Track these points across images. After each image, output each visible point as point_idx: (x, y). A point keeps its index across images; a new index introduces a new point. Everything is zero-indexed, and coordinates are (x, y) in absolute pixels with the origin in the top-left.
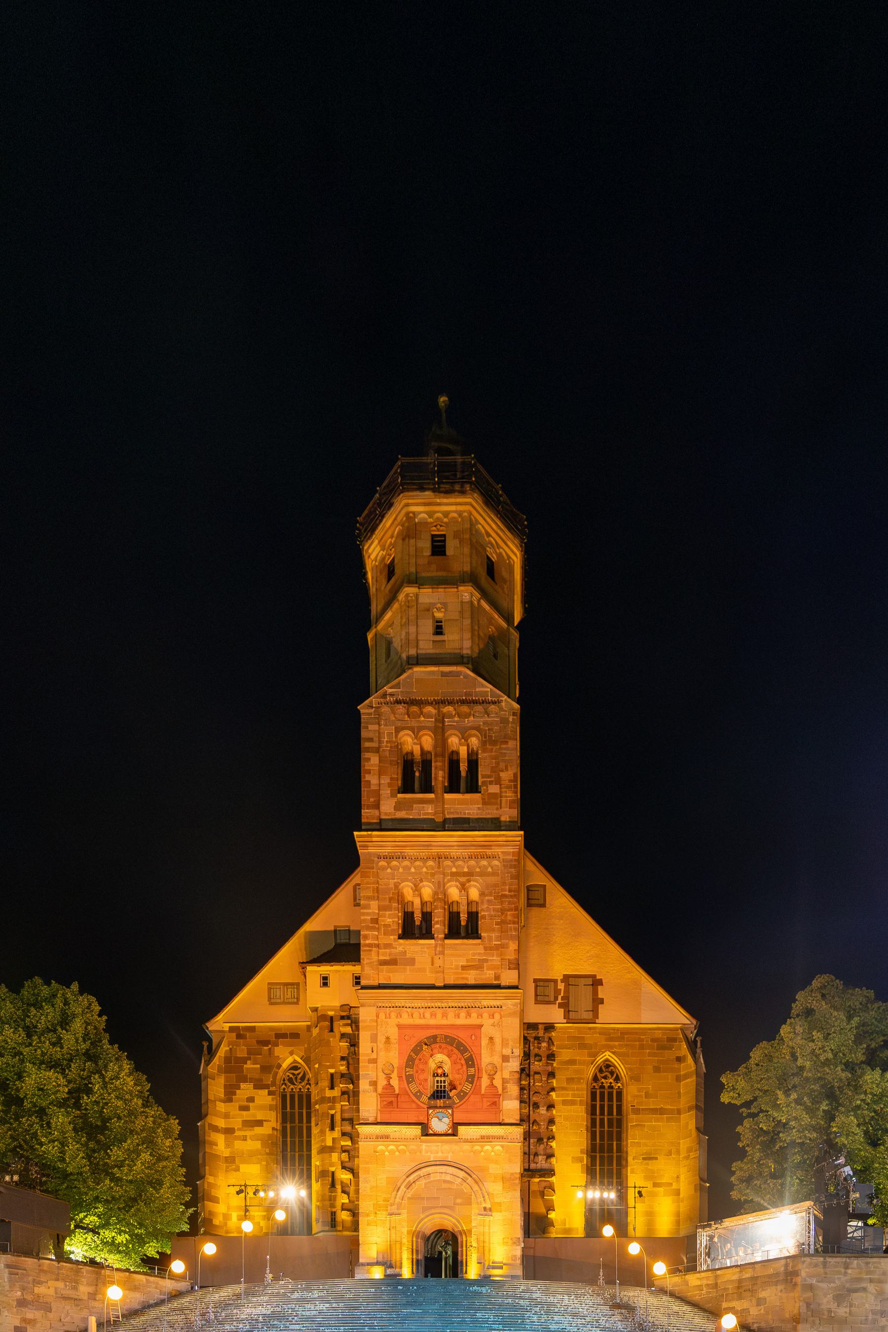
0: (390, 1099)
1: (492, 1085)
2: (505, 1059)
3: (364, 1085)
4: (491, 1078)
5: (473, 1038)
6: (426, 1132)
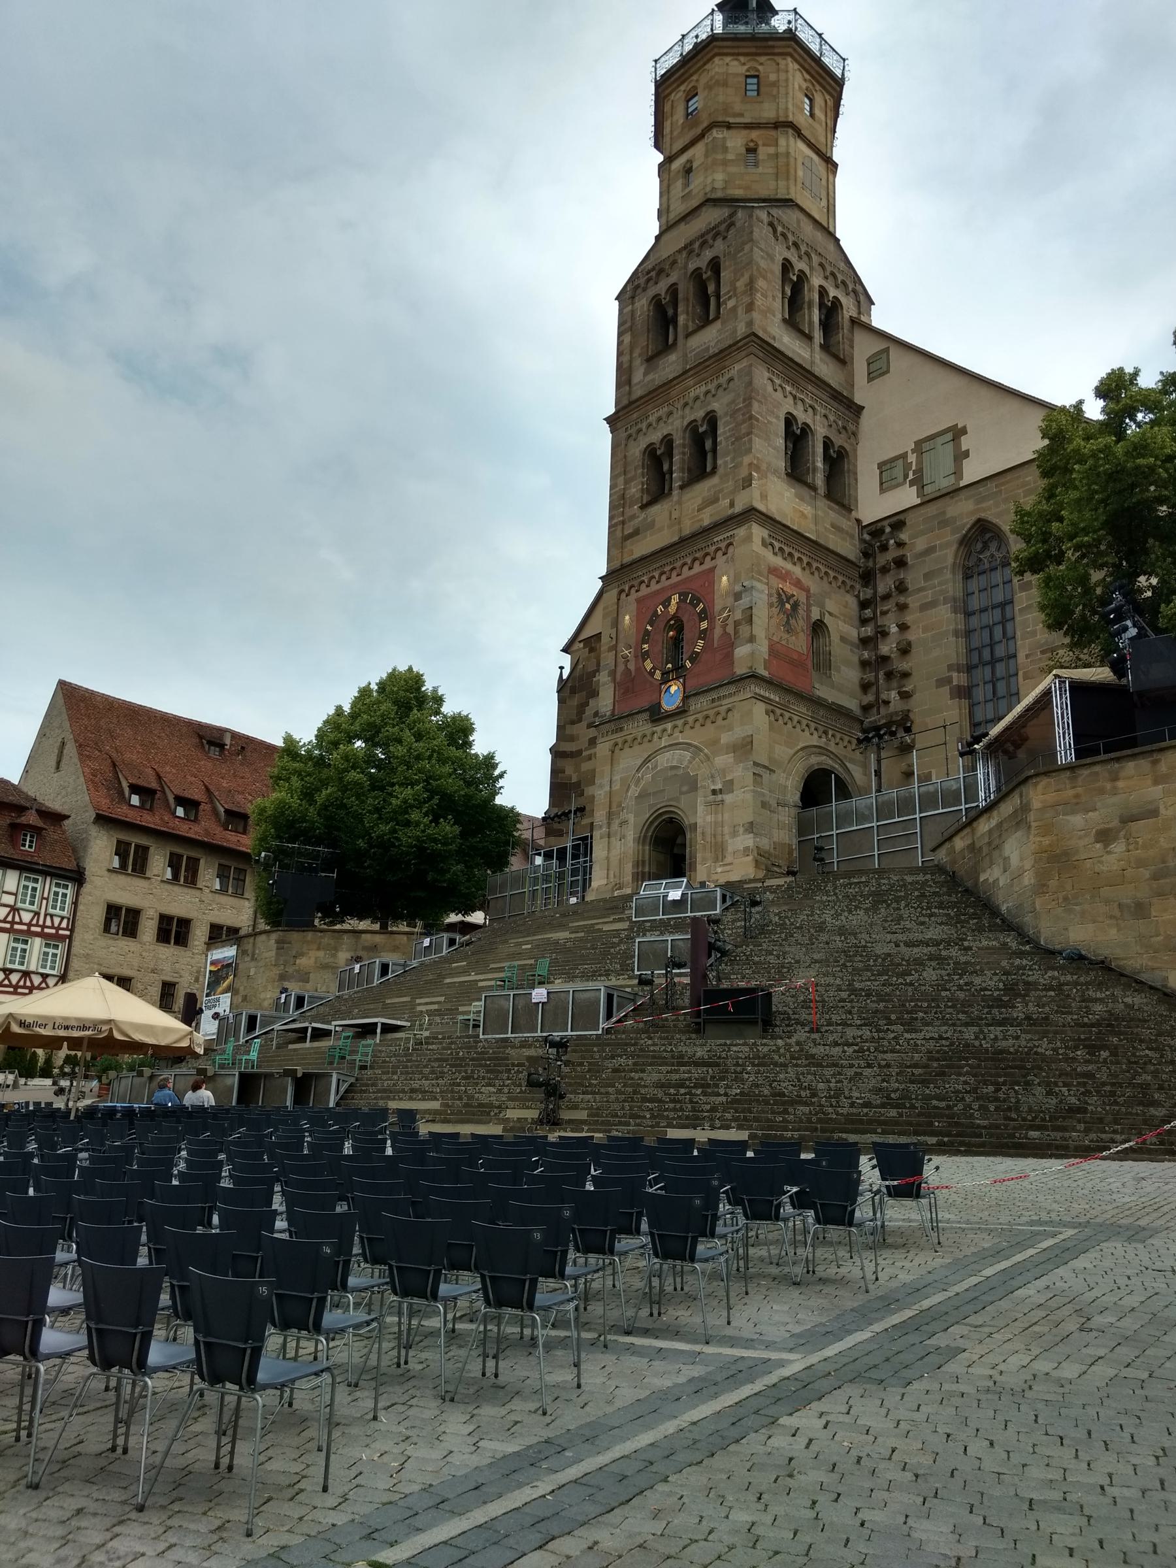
1: (725, 633)
4: (725, 626)
6: (656, 715)
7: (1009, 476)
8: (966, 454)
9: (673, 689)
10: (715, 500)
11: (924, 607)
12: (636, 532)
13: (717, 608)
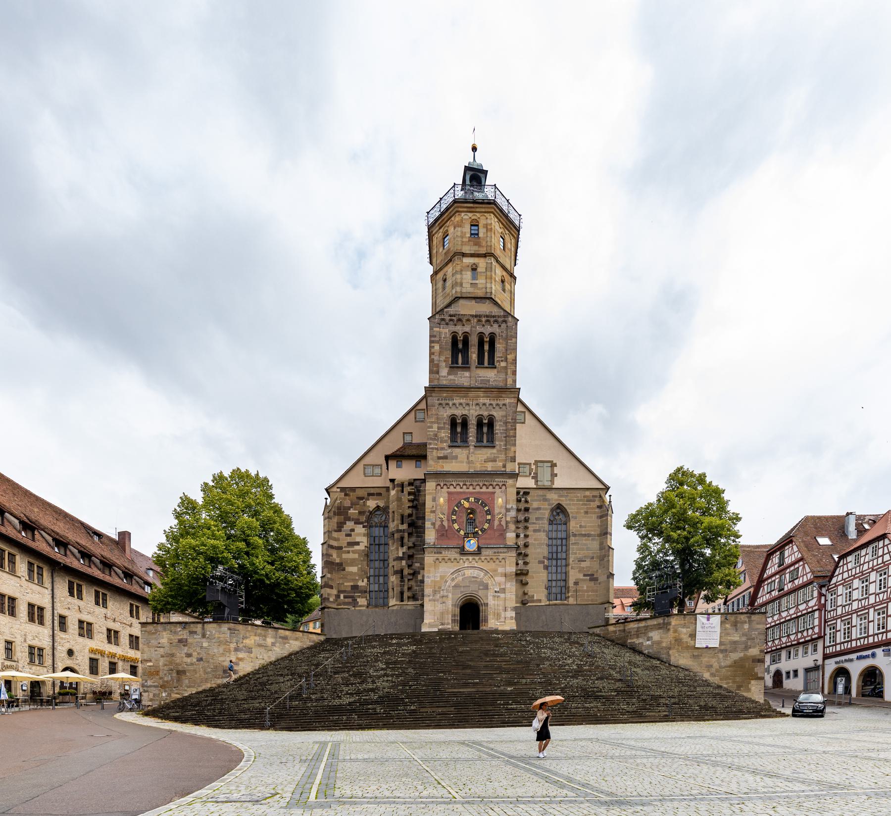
0: (443, 533)
2: (508, 510)
6: (463, 552)
9: (472, 542)
10: (495, 461)
12: (445, 458)
13: (497, 511)
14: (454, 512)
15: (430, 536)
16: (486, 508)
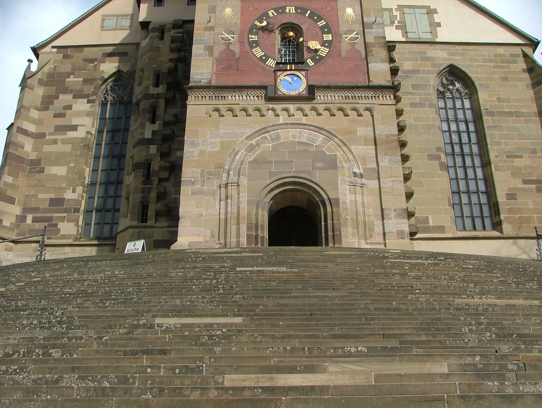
3: (197, 49)
5: (328, 9)
7: (471, 47)
8: (439, 25)
11: (413, 105)
14: (253, 30)
15: (201, 69)
16: (322, 23)
